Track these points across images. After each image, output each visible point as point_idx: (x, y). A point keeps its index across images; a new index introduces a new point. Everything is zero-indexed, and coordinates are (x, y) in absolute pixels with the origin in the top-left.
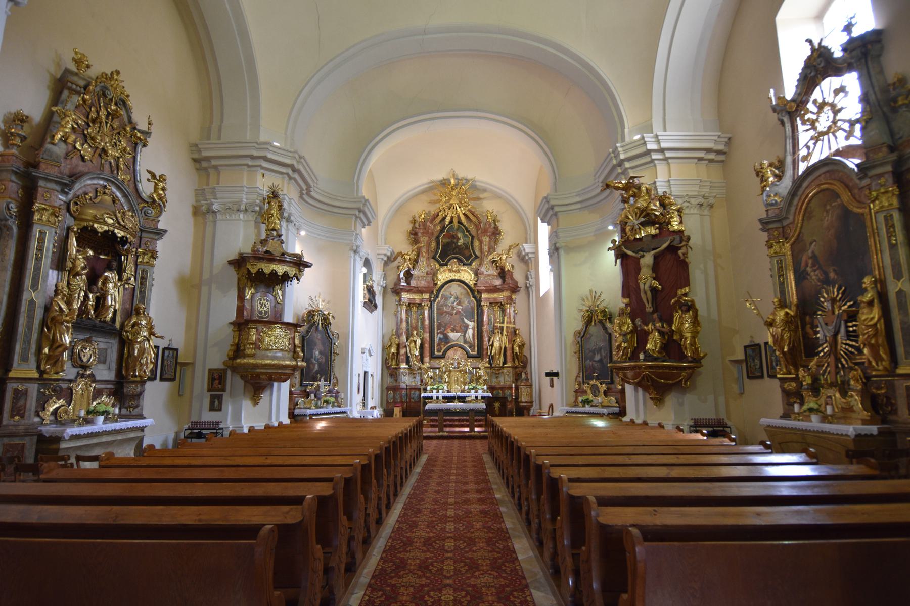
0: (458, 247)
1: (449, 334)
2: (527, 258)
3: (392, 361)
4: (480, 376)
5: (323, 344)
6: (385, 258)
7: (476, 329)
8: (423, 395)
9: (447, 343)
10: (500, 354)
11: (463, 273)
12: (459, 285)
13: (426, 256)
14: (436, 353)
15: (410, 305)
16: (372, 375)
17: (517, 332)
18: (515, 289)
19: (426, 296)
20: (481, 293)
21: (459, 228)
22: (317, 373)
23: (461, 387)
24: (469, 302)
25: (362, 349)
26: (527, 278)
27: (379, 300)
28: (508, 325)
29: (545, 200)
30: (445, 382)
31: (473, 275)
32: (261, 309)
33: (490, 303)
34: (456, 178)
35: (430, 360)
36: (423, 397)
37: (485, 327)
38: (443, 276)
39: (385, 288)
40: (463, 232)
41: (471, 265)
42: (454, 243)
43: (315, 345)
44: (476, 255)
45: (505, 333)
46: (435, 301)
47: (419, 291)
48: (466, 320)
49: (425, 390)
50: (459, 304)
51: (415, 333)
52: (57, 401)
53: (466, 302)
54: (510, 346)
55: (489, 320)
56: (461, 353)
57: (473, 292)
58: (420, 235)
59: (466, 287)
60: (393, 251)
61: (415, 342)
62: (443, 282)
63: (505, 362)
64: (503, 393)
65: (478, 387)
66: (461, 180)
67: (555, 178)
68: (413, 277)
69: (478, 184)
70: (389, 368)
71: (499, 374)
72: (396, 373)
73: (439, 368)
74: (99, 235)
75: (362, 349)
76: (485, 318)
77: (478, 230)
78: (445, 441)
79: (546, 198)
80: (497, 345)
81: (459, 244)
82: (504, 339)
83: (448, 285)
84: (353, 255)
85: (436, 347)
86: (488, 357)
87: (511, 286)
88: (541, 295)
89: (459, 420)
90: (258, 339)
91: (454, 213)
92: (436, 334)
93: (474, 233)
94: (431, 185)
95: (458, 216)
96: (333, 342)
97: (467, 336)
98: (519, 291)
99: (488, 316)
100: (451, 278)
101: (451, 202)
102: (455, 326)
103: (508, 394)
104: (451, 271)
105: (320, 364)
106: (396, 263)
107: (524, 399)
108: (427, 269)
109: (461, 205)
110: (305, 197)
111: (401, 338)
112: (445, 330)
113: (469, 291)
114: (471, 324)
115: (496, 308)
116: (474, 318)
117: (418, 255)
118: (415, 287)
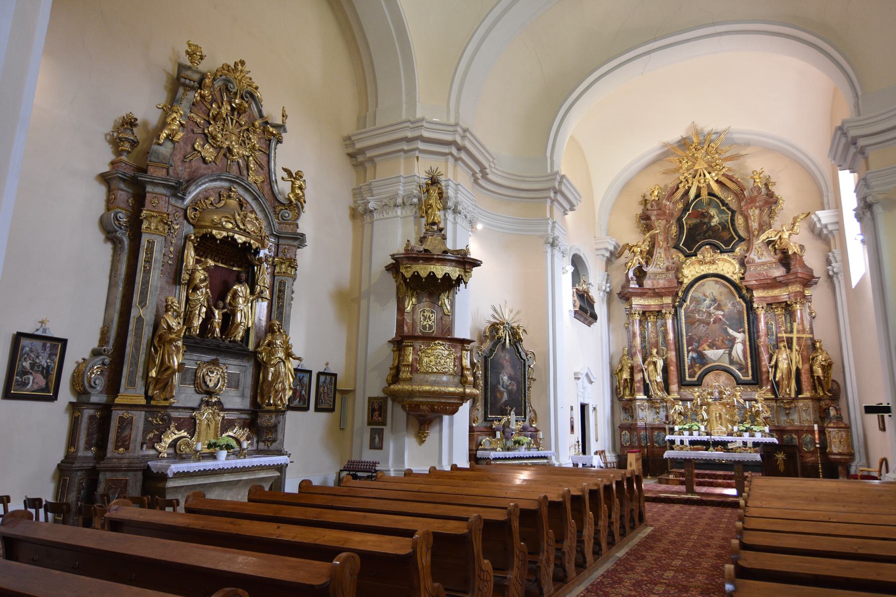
0: (710, 228)
1: (705, 352)
2: (825, 231)
3: (624, 389)
4: (758, 413)
5: (513, 367)
6: (608, 254)
7: (748, 343)
8: (668, 437)
9: (704, 365)
10: (789, 378)
11: (720, 264)
12: (717, 282)
13: (665, 245)
14: (687, 379)
15: (644, 314)
16: (595, 409)
17: (818, 345)
18: (808, 281)
19: (668, 300)
20: (752, 291)
21: (710, 203)
22: (506, 404)
23: (727, 427)
24: (733, 305)
25: (575, 374)
26: (829, 262)
27: (600, 308)
29: (839, 132)
30: (703, 420)
31: (737, 266)
32: (425, 323)
33: (768, 304)
34: (698, 133)
35: (680, 388)
36: (669, 440)
37: (763, 340)
38: (690, 271)
39: (609, 294)
40: (718, 207)
41: (734, 252)
42: (705, 223)
43: (503, 367)
44: (739, 237)
45: (795, 346)
46: (681, 306)
47: (657, 294)
48: (730, 331)
49: (672, 431)
50: (719, 308)
51: (654, 351)
52: (176, 432)
53: (729, 305)
54: (807, 366)
55: (768, 329)
56: (727, 379)
57: (740, 290)
58: (653, 218)
59: (727, 283)
60: (617, 244)
61: (655, 364)
63: (799, 391)
64: (799, 438)
65: (755, 428)
66: (709, 134)
67: (857, 96)
68: (648, 275)
69: (735, 136)
70: (620, 399)
71: (790, 409)
72: (631, 407)
73: (691, 400)
74: (218, 242)
75: (575, 374)
76: (762, 325)
77: (740, 202)
78: (694, 508)
79: (840, 128)
80: (783, 365)
81: (712, 224)
82: (795, 356)
83: (699, 283)
84: (549, 250)
85: (687, 370)
86: (770, 384)
87: (800, 275)
88: (854, 285)
89: (725, 477)
90: (415, 360)
91: (702, 181)
92: (686, 352)
93: (733, 206)
94: (666, 149)
95: (709, 185)
96: (527, 364)
97: (734, 353)
98: (816, 283)
99: (766, 323)
100: (703, 273)
101: (696, 168)
103: (808, 440)
104: (701, 262)
105: (510, 393)
106: (622, 260)
107: (836, 448)
108: (667, 264)
109: (710, 169)
110: (481, 182)
111: (634, 359)
112: (698, 347)
113: (732, 289)
114: (739, 337)
115: (779, 311)
116: (742, 326)
117: (653, 245)
118: (650, 289)
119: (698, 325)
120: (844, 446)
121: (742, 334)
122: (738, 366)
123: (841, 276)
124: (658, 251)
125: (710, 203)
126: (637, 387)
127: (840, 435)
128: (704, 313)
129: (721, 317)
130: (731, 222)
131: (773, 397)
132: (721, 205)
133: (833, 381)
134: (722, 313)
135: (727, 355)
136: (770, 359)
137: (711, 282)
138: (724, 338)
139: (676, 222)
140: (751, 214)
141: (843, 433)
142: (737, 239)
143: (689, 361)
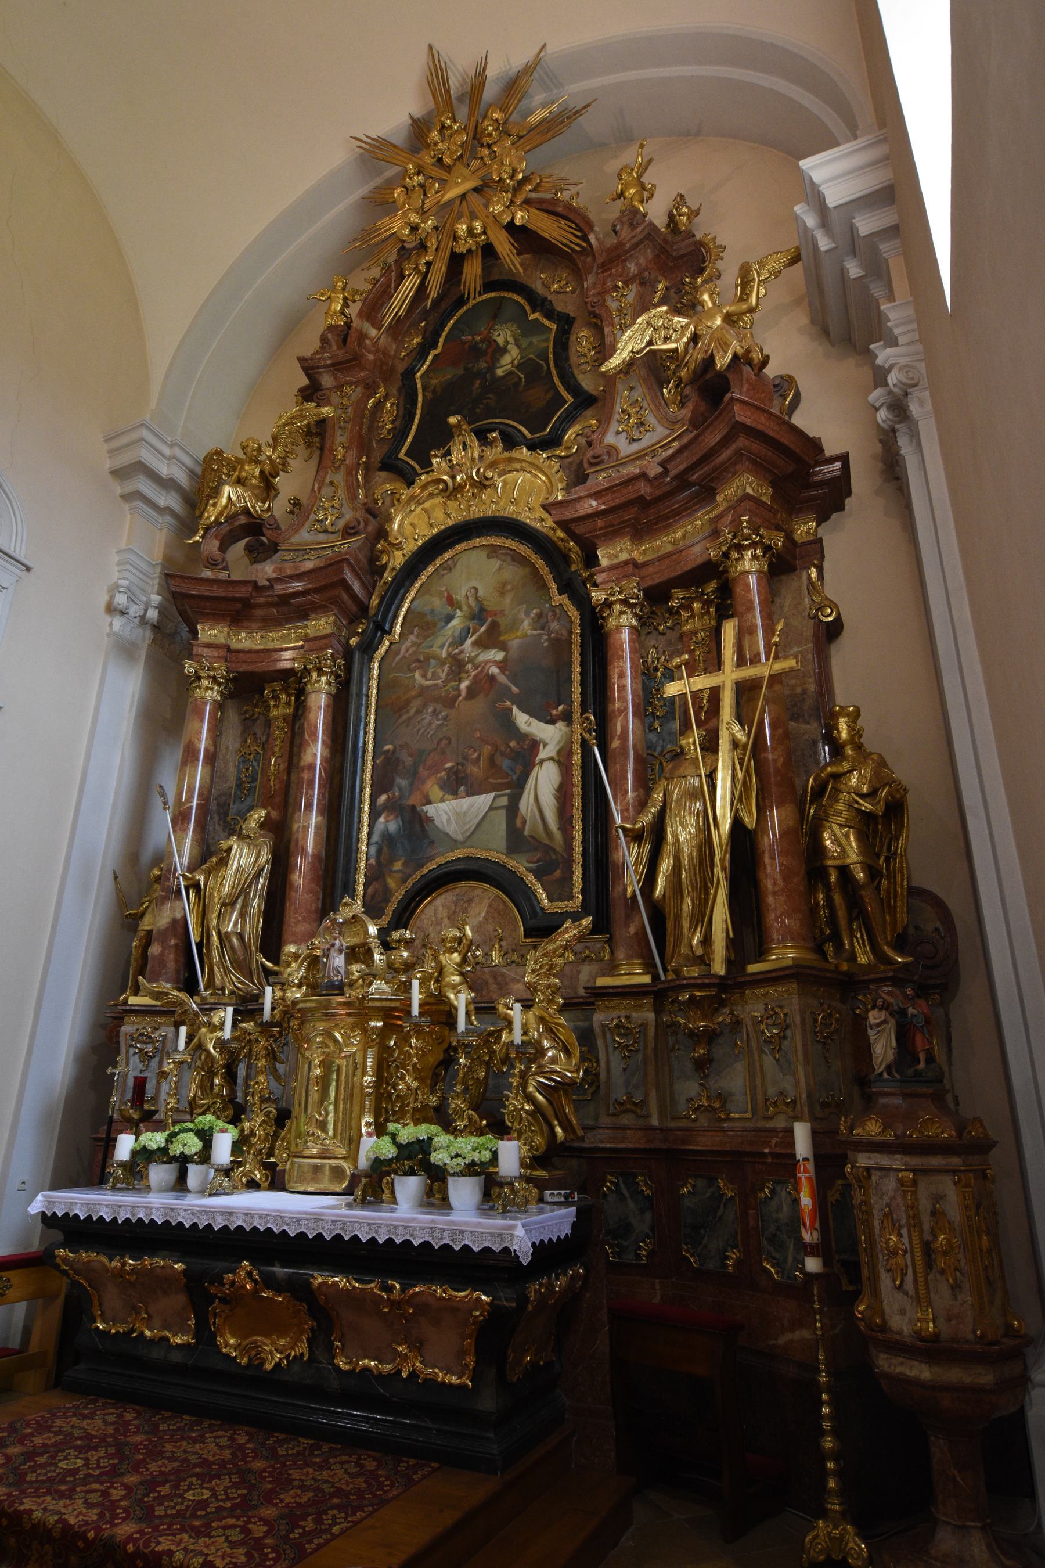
1: (430, 810)
2: (854, 270)
12: (493, 551)
28: (749, 672)
44: (575, 389)
46: (368, 648)
48: (522, 719)
53: (526, 623)
56: (496, 913)
59: (525, 550)
62: (411, 547)
81: (500, 372)
91: (462, 228)
97: (526, 804)
102: (466, 758)
108: (348, 516)
113: (540, 563)
119: (418, 712)
120: (955, 1288)
121: (561, 725)
122: (538, 855)
123: (921, 403)
124: (328, 480)
125: (496, 312)
126: (154, 957)
127: (925, 1205)
128: (442, 662)
129: (494, 670)
130: (555, 353)
131: (647, 979)
132: (528, 308)
133: (914, 892)
134: (500, 656)
135: (503, 812)
136: (642, 805)
137: (475, 553)
138: (496, 749)
139: (399, 390)
140: (613, 305)
141: (948, 1186)
142: (570, 400)
143: (373, 850)
